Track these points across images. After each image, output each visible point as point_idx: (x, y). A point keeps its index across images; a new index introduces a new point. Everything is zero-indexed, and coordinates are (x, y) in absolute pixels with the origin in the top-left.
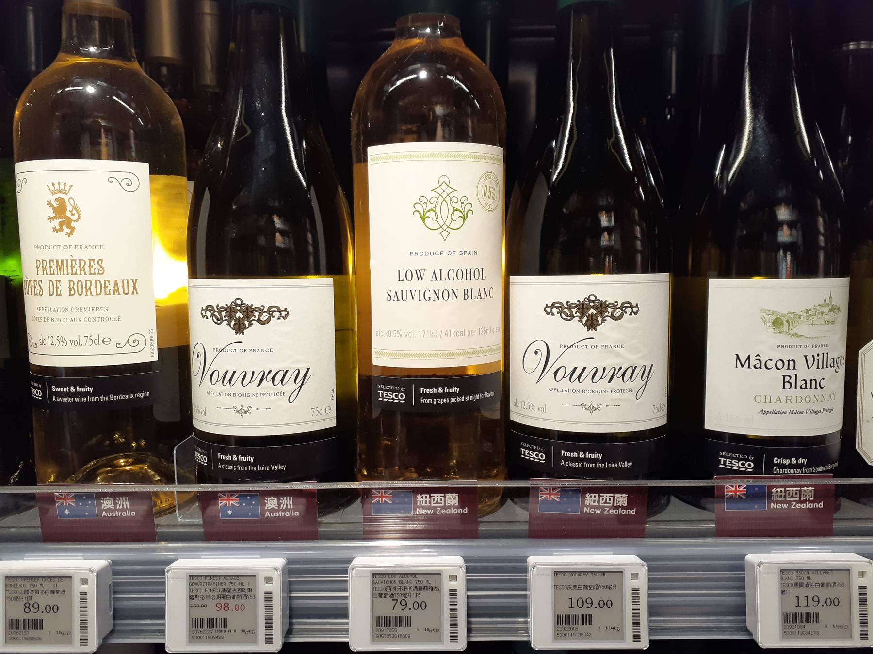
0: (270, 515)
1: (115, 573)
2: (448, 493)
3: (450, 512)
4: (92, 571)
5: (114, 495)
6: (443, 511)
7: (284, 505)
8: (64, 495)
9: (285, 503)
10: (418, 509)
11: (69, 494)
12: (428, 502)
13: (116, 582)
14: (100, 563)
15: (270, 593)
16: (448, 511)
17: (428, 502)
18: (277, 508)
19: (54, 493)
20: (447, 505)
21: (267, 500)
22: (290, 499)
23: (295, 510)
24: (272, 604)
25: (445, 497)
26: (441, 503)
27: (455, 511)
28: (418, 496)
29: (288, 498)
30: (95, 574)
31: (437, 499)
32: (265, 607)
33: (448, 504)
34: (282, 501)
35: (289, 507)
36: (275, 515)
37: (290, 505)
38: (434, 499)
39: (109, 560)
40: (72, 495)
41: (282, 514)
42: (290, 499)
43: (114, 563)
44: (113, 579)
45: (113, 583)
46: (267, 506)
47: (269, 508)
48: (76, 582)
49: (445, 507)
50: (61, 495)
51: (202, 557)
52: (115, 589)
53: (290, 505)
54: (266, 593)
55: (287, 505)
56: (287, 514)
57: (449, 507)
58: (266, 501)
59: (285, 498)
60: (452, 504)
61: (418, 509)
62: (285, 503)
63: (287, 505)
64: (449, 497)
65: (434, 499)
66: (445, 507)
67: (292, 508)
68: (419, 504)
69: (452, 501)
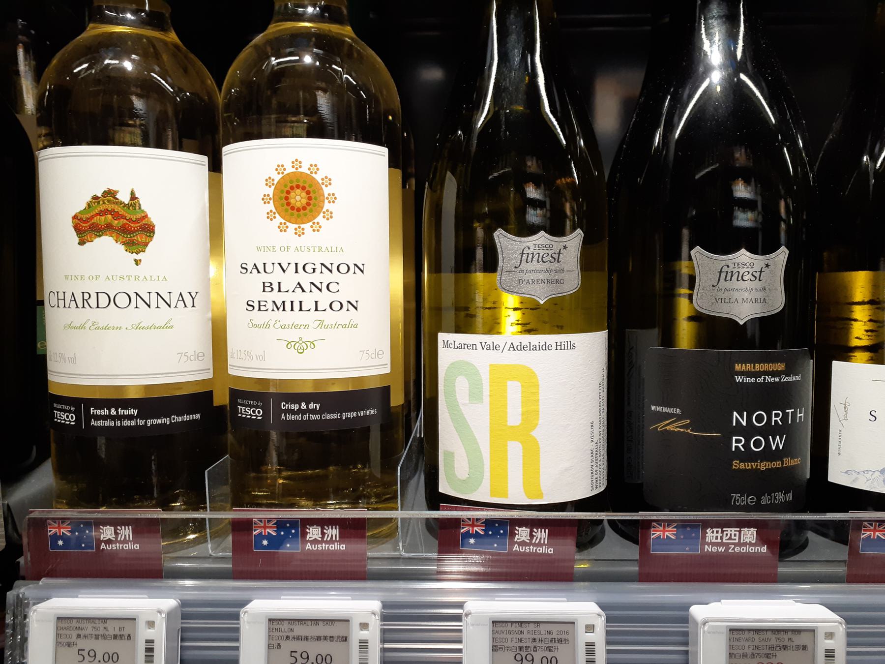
0: (519, 549)
1: (185, 616)
2: (744, 528)
3: (745, 551)
4: (160, 612)
5: (323, 523)
6: (737, 549)
7: (537, 538)
8: (265, 521)
9: (539, 537)
10: (706, 546)
11: (269, 520)
12: (719, 538)
13: (184, 627)
14: (169, 603)
15: (593, 644)
16: (743, 549)
17: (719, 538)
18: (528, 541)
19: (253, 519)
20: (742, 541)
21: (518, 531)
22: (545, 532)
23: (549, 545)
24: (595, 659)
25: (740, 532)
26: (735, 539)
27: (752, 550)
28: (708, 531)
29: (543, 530)
30: (163, 616)
31: (731, 534)
32: (587, 661)
33: (744, 540)
34: (536, 533)
35: (542, 542)
36: (525, 549)
37: (544, 539)
38: (727, 534)
39: (178, 600)
40: (274, 522)
41: (533, 549)
42: (545, 532)
43: (184, 604)
44: (182, 623)
45: (182, 628)
46: (517, 537)
47: (518, 541)
48: (141, 625)
49: (740, 544)
50: (261, 521)
51: (496, 599)
52: (185, 634)
53: (544, 539)
54: (588, 644)
55: (541, 539)
56: (539, 550)
57: (745, 544)
58: (516, 532)
59: (539, 530)
60: (748, 540)
61: (706, 546)
62: (539, 537)
63: (541, 539)
64: (745, 532)
65: (727, 534)
66: (740, 544)
67: (546, 543)
68: (708, 540)
69: (749, 537)
